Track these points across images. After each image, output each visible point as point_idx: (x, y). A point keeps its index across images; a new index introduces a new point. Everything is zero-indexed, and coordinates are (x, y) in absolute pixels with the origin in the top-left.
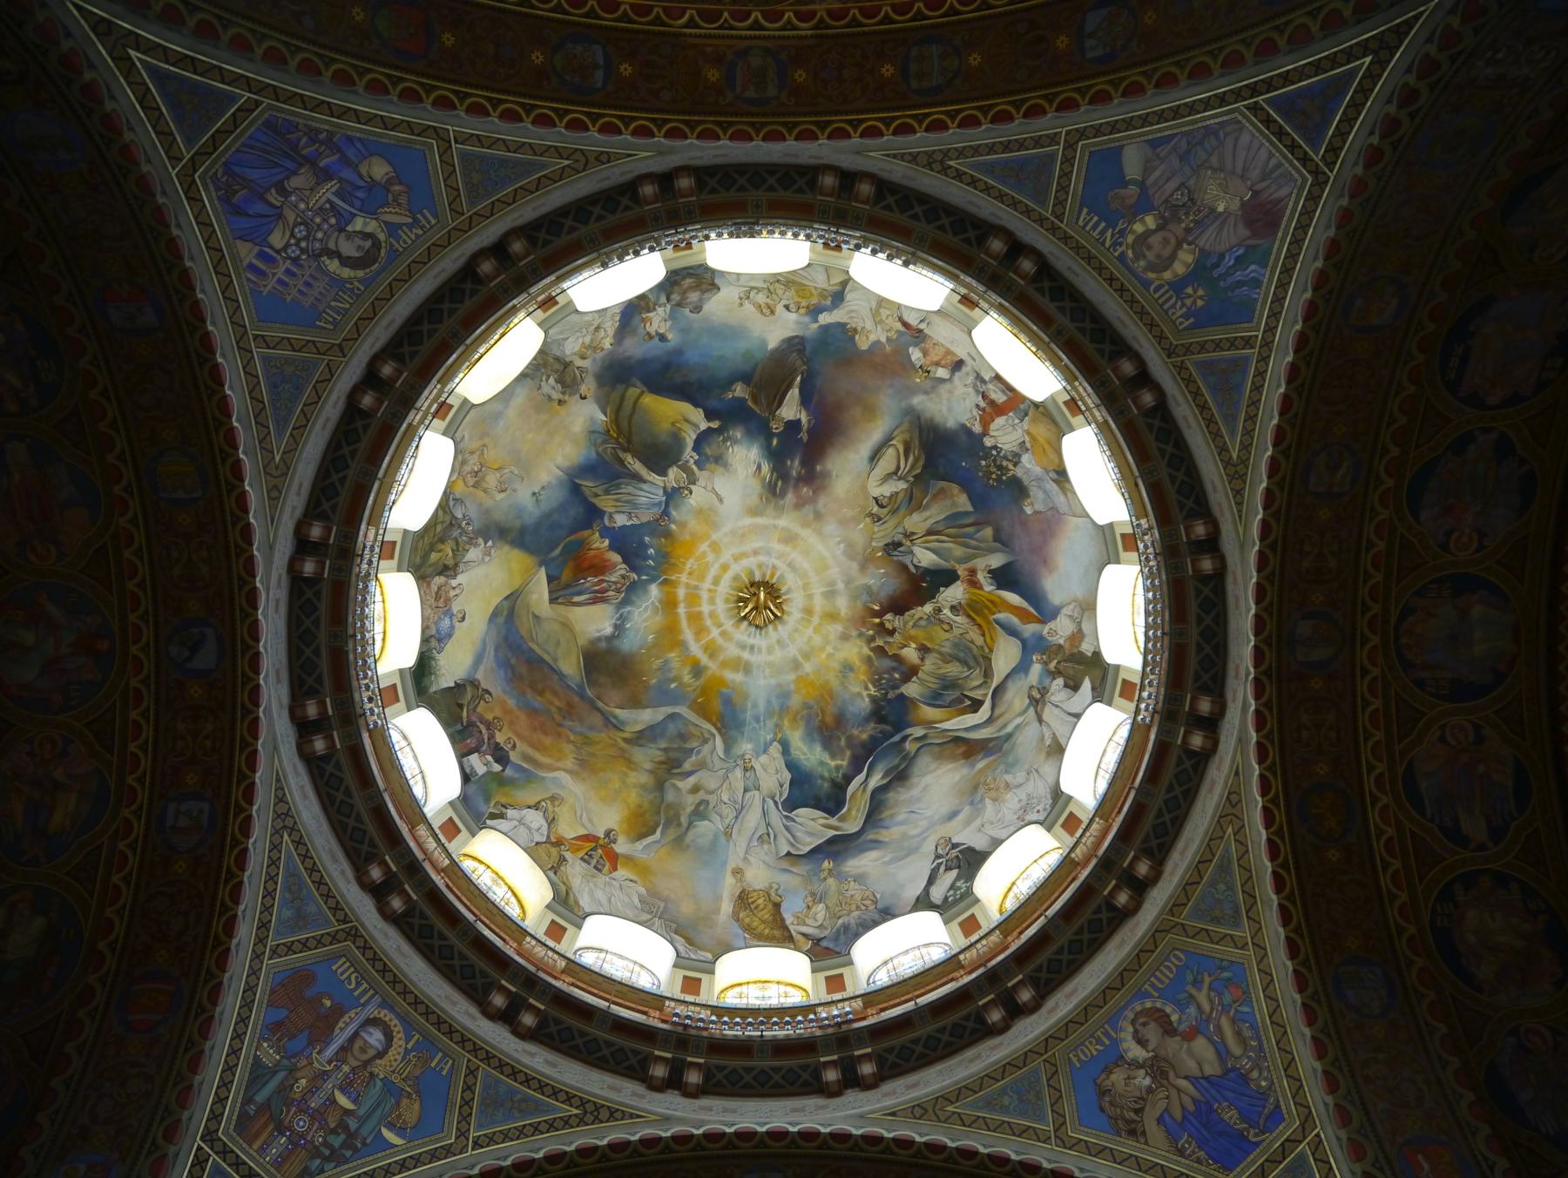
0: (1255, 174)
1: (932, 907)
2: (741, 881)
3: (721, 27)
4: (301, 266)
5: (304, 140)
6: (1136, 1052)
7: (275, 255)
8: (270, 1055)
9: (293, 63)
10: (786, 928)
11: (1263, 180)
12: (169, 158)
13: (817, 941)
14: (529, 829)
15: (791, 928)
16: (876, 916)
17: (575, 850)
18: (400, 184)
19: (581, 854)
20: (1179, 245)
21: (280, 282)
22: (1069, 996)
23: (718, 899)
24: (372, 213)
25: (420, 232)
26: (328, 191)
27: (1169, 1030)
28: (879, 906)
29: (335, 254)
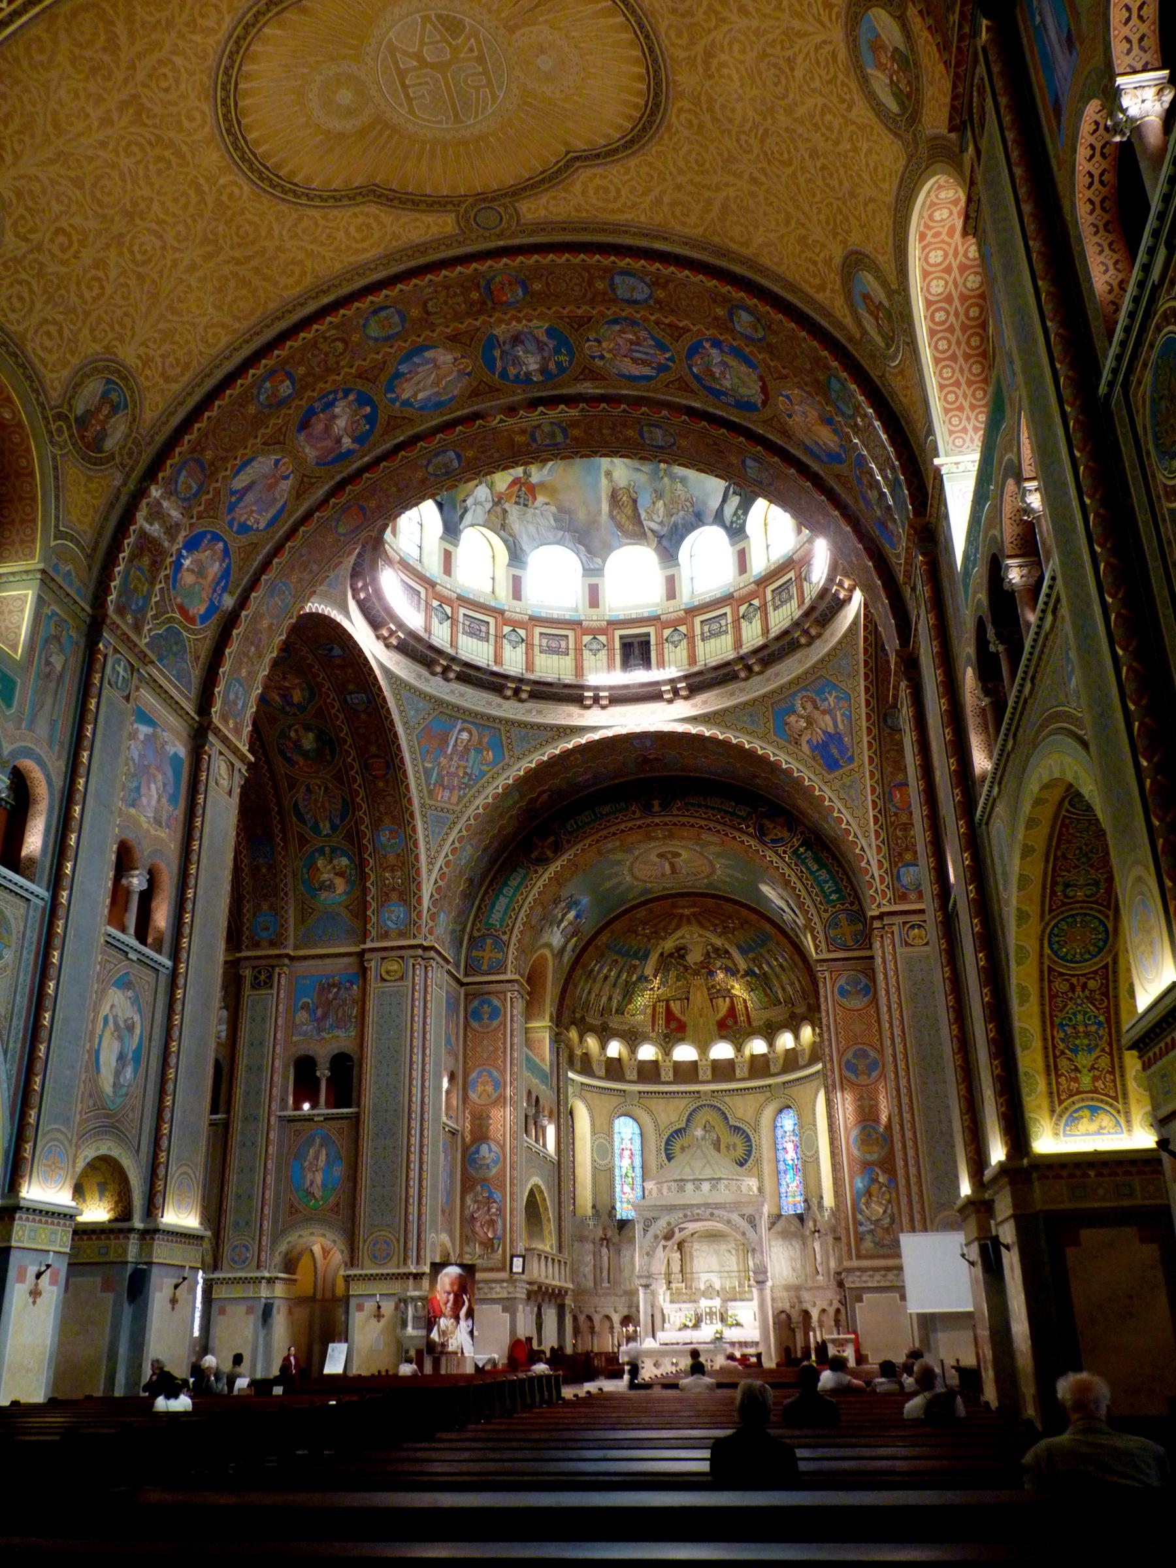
2: (611, 480)
8: (429, 765)
10: (640, 523)
14: (481, 504)
17: (509, 496)
19: (514, 499)
22: (777, 675)
23: (599, 502)
27: (816, 707)
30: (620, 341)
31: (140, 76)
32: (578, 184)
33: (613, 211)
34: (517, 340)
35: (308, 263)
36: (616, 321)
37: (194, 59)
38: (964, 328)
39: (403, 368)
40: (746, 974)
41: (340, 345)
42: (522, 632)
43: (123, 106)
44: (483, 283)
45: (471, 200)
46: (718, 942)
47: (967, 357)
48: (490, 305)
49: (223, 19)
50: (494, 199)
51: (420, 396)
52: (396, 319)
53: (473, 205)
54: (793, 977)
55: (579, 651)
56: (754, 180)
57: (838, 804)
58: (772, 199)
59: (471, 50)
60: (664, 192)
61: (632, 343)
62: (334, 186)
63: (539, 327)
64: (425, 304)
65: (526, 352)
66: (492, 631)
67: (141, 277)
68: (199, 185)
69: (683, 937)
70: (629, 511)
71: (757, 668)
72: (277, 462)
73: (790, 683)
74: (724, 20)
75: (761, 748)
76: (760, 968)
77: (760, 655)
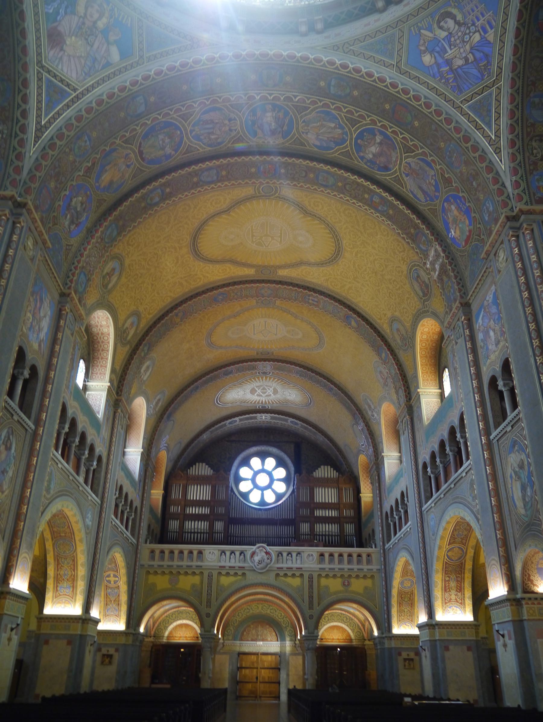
0: (65, 59)
3: (284, 94)
4: (472, 21)
5: (451, 81)
7: (481, 30)
9: (444, 116)
11: (61, 57)
12: (501, 90)
18: (421, 50)
20: (85, 14)
21: (483, 16)
24: (436, 40)
25: (419, 24)
26: (450, 53)
29: (457, 23)
36: (219, 144)
41: (347, 187)
45: (272, 197)
50: (263, 196)
51: (333, 125)
52: (320, 178)
53: (272, 195)
56: (159, 242)
61: (212, 133)
64: (306, 176)
72: (407, 175)
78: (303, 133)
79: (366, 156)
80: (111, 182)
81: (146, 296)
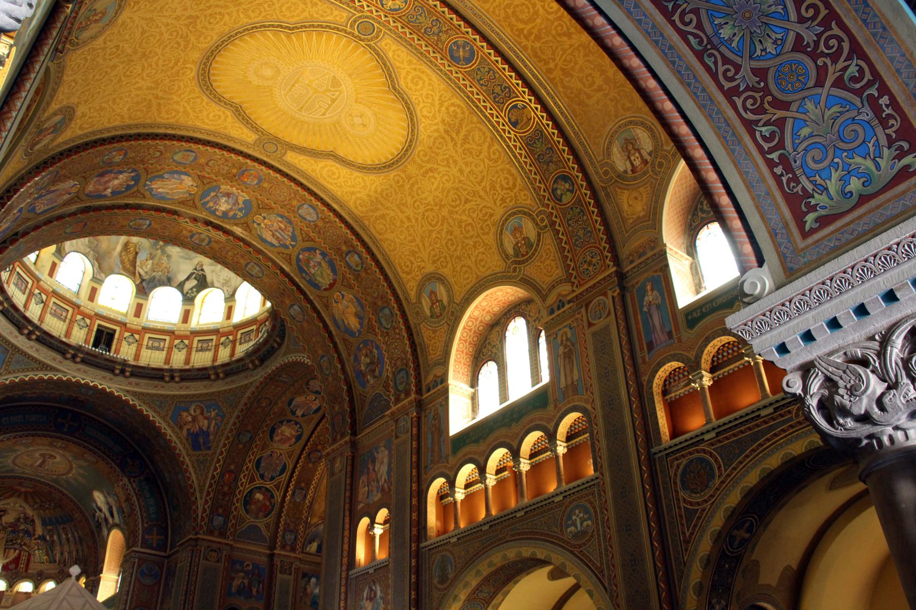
1: (182, 292)
6: (193, 413)
10: (135, 267)
13: (143, 280)
15: (137, 268)
16: (165, 280)
22: (188, 388)
28: (169, 275)
30: (275, 224)
31: (209, 12)
32: (324, 163)
33: (328, 182)
34: (228, 195)
35: (180, 114)
36: (282, 217)
37: (232, 21)
38: (475, 332)
39: (166, 176)
40: (39, 538)
41: (158, 154)
42: (44, 297)
43: (191, 17)
44: (244, 169)
46: (30, 512)
47: (470, 343)
48: (237, 178)
49: (258, 17)
51: (160, 190)
54: (73, 548)
55: (72, 322)
56: (408, 218)
57: (191, 469)
58: (412, 230)
59: (333, 95)
60: (359, 192)
61: (280, 228)
62: (225, 96)
63: (243, 197)
65: (225, 201)
66: (29, 286)
67: (120, 80)
68: (179, 61)
69: (9, 504)
70: (131, 257)
71: (177, 379)
72: (76, 185)
73: (194, 395)
74: (449, 167)
75: (159, 422)
76: (51, 536)
77: (182, 374)
78: (197, 187)
79: (126, 174)
80: (357, 315)
81: (481, 211)
